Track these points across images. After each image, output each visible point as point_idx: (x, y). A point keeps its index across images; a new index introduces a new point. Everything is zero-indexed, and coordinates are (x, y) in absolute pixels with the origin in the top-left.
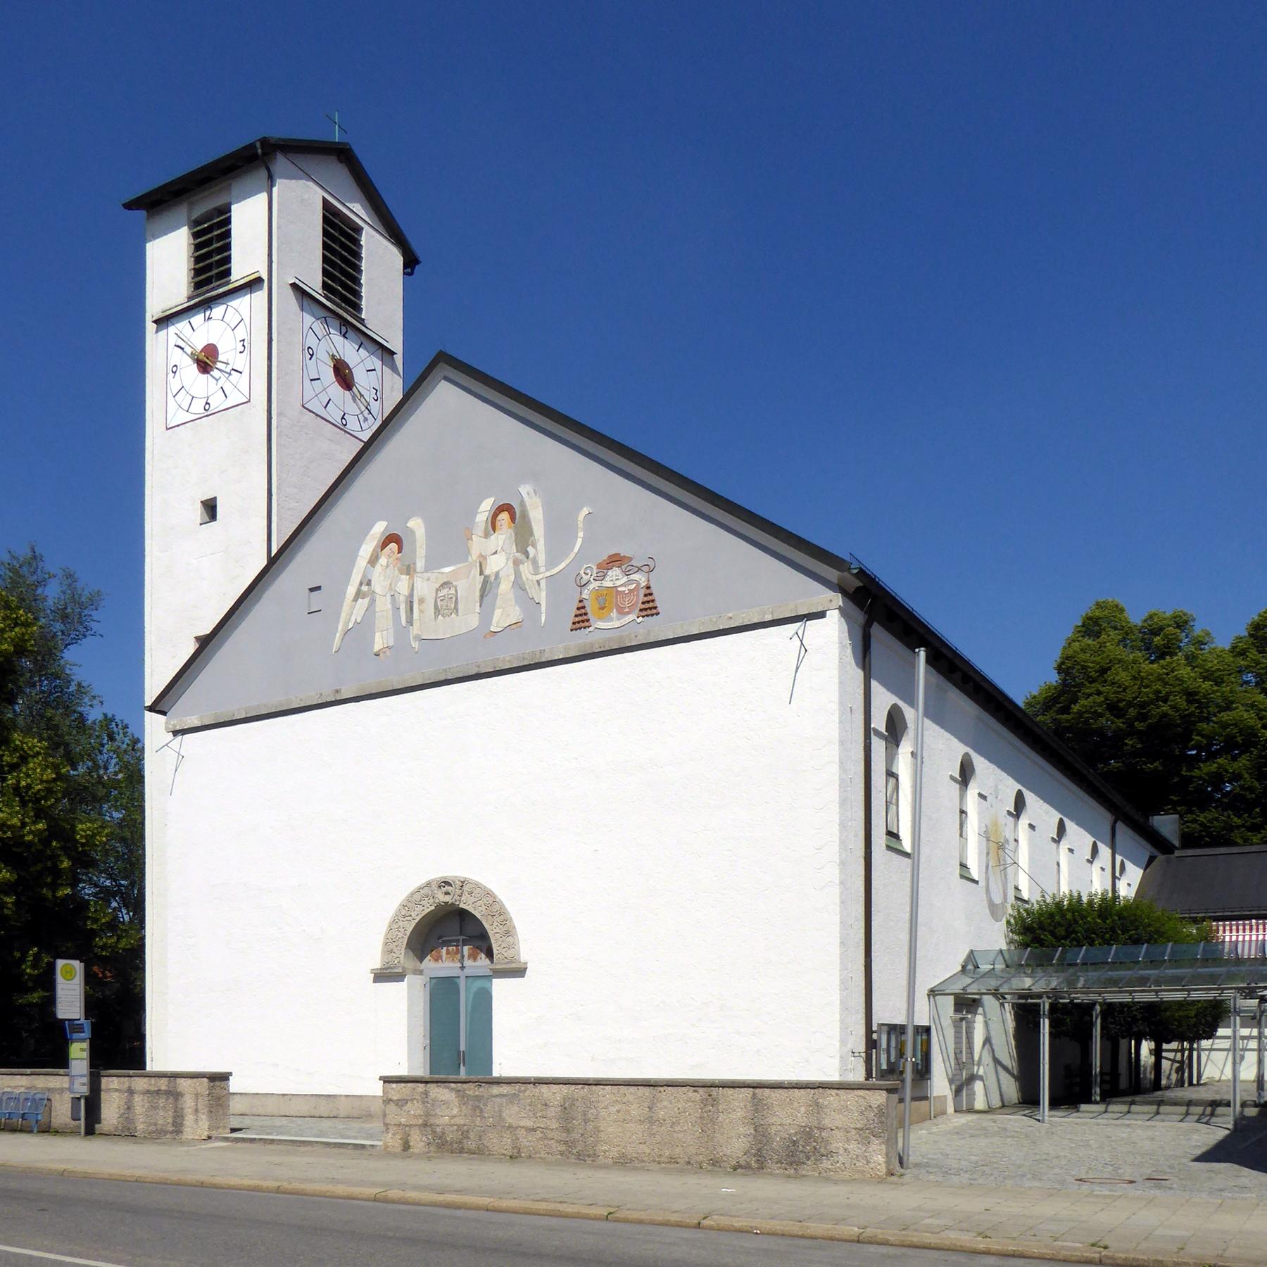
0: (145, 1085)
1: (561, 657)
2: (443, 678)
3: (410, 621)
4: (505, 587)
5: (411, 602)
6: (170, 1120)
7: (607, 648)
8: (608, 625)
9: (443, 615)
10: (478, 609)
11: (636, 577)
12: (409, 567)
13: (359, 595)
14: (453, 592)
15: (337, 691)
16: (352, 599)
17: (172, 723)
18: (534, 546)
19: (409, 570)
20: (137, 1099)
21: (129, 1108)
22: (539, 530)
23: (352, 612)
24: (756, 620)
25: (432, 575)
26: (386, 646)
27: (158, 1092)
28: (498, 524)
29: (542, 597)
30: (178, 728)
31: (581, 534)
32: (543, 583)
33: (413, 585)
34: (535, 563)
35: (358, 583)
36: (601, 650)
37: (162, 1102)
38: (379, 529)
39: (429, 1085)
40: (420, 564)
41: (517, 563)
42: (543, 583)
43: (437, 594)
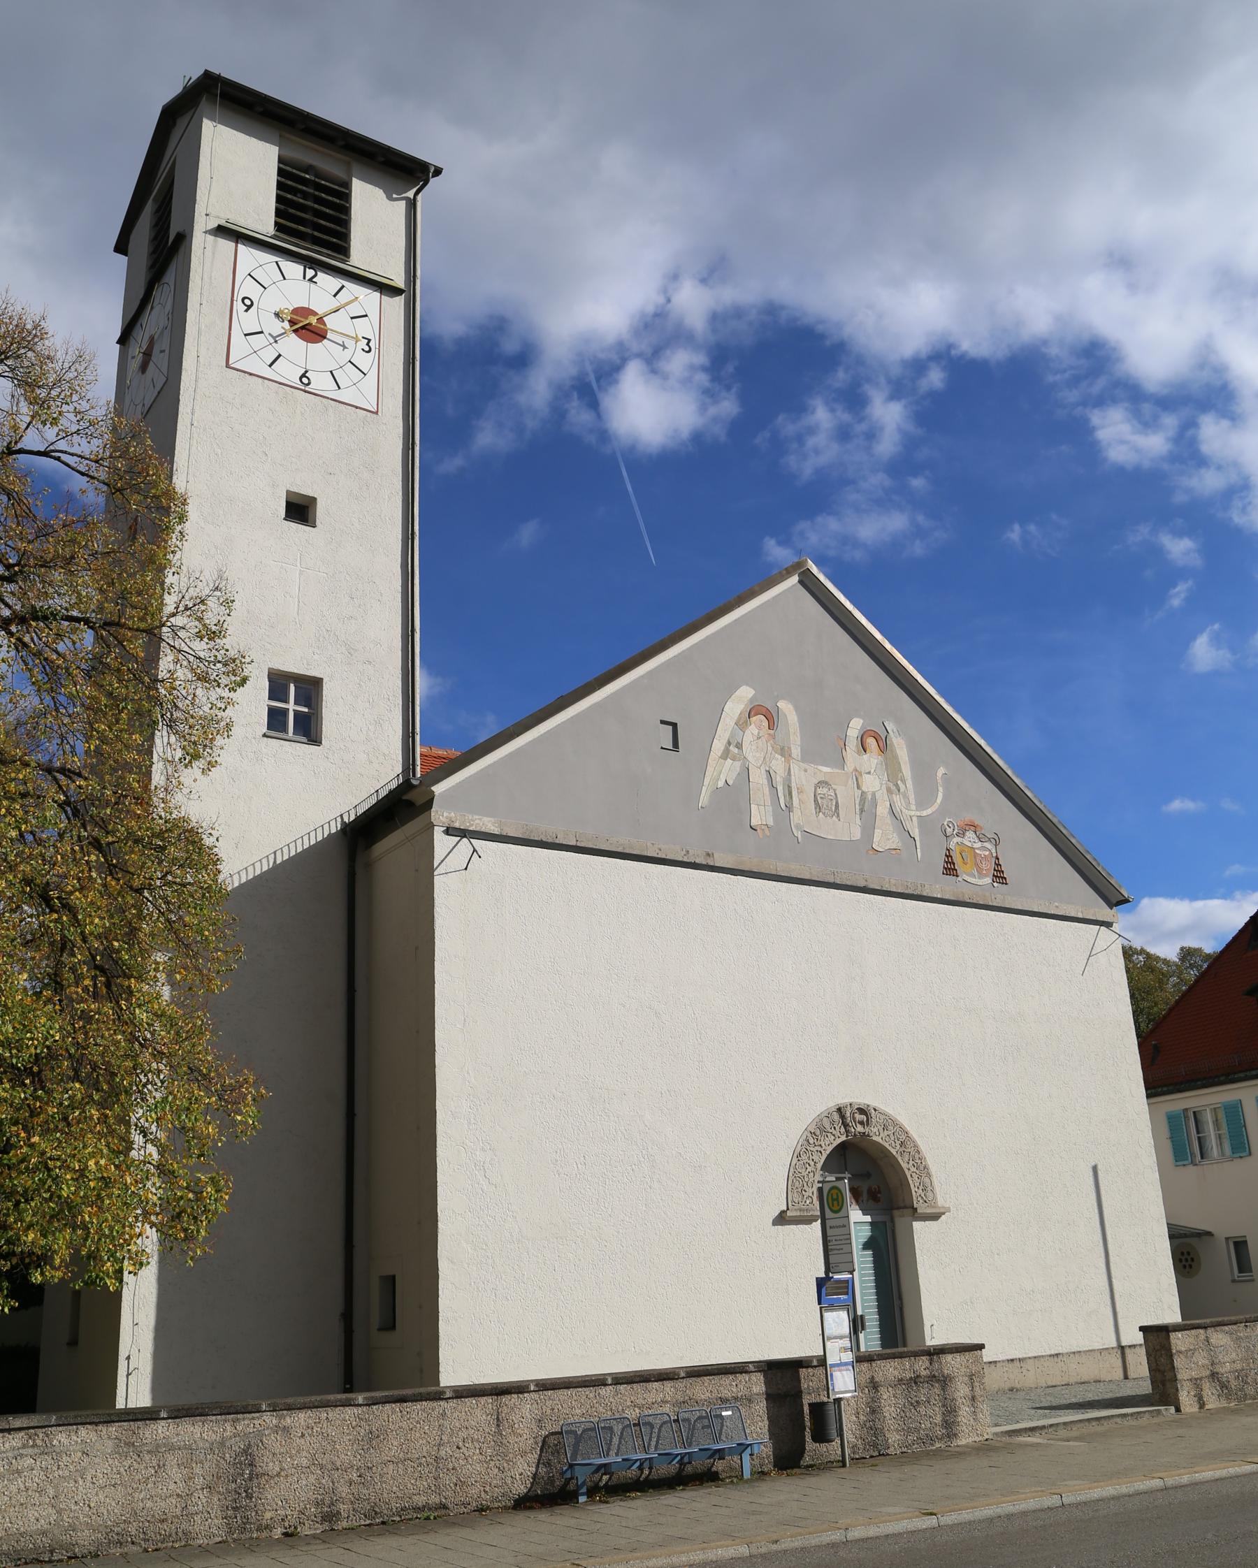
0: (896, 1373)
1: (939, 896)
2: (831, 880)
3: (789, 808)
4: (882, 810)
5: (789, 787)
6: (938, 1419)
7: (975, 901)
8: (976, 881)
9: (824, 814)
10: (858, 822)
11: (988, 845)
12: (782, 749)
13: (726, 755)
14: (833, 794)
15: (708, 855)
16: (719, 755)
17: (445, 814)
18: (904, 781)
19: (784, 752)
20: (886, 1394)
21: (873, 1411)
22: (906, 771)
23: (720, 772)
24: (1073, 914)
25: (811, 768)
26: (764, 823)
27: (916, 1380)
28: (867, 746)
29: (916, 833)
30: (457, 825)
31: (941, 789)
32: (915, 819)
33: (789, 769)
34: (905, 797)
35: (725, 742)
36: (971, 901)
37: (923, 1393)
38: (745, 694)
39: (1210, 1330)
40: (796, 752)
41: (889, 791)
42: (915, 819)
43: (815, 789)
